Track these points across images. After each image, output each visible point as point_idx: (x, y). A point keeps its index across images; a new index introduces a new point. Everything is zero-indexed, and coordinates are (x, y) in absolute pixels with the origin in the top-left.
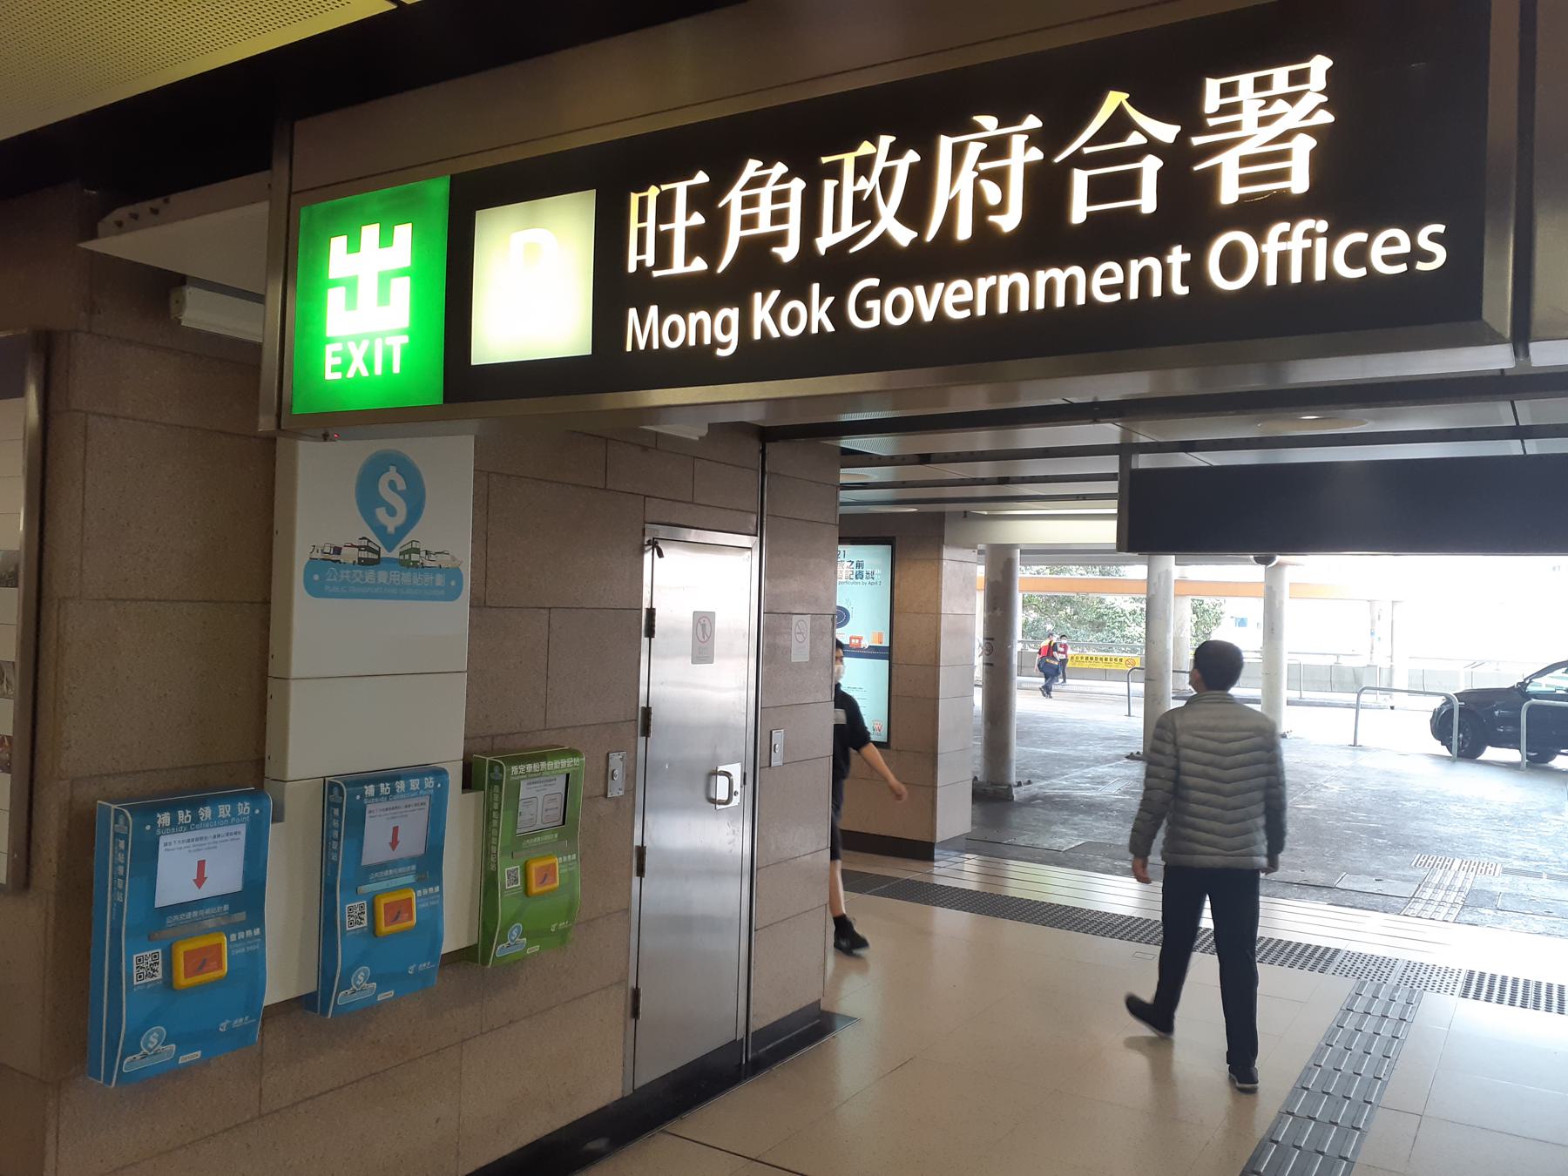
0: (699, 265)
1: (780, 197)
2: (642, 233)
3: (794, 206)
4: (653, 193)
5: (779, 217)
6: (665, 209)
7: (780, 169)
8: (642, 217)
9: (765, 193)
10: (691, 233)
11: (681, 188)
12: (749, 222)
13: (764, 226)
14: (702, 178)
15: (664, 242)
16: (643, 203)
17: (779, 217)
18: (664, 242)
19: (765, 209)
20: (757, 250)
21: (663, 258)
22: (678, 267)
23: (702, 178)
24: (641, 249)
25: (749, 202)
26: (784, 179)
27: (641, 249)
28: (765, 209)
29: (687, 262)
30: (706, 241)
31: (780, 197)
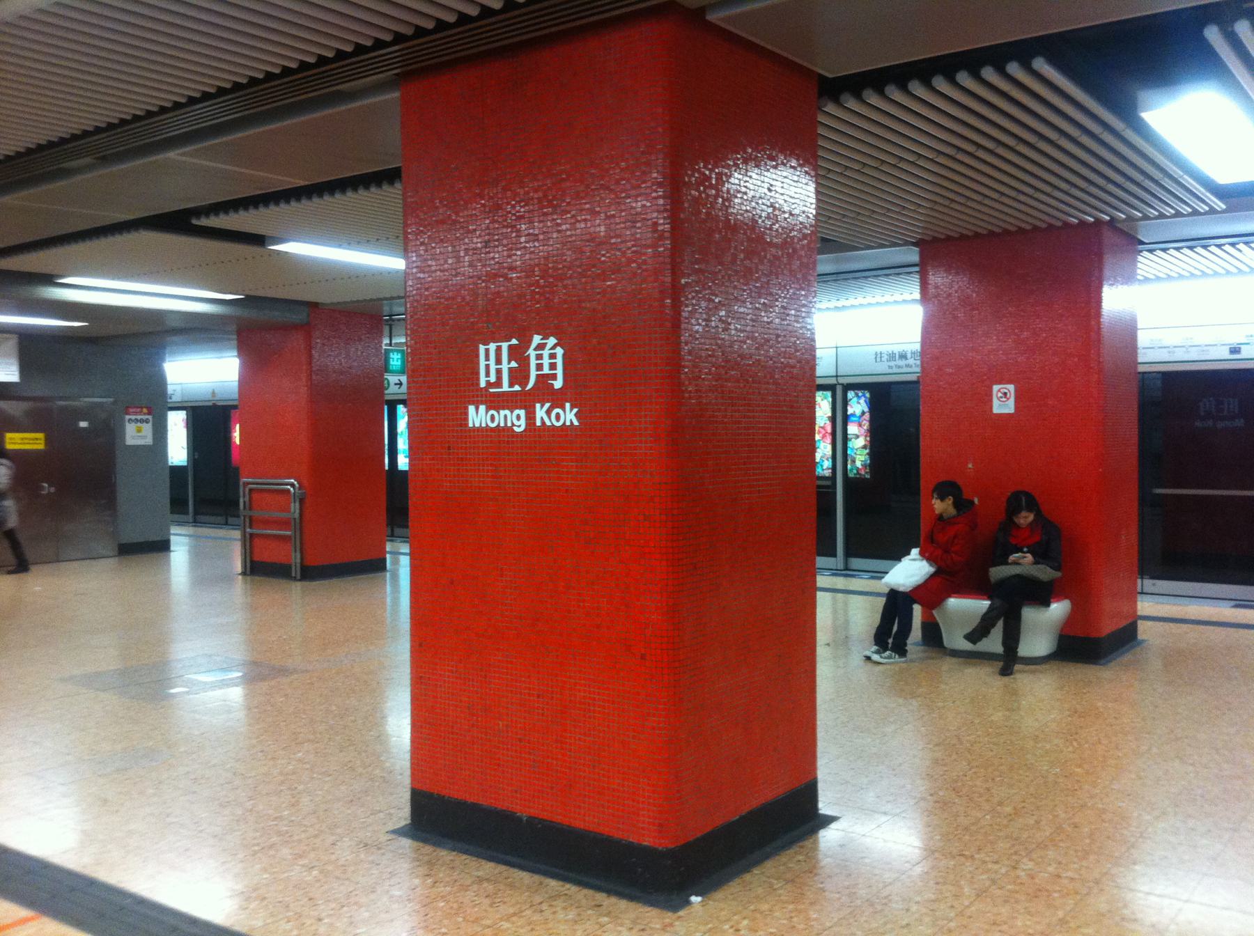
0: (517, 388)
1: (553, 356)
2: (487, 367)
3: (559, 361)
4: (492, 347)
5: (553, 366)
7: (552, 341)
8: (487, 359)
9: (546, 353)
10: (511, 370)
11: (505, 345)
12: (539, 367)
13: (546, 370)
14: (514, 341)
15: (499, 372)
16: (487, 351)
17: (553, 366)
18: (499, 372)
19: (546, 362)
20: (543, 380)
21: (499, 383)
22: (505, 387)
23: (514, 341)
24: (488, 375)
25: (539, 357)
26: (554, 347)
27: (488, 375)
28: (546, 362)
29: (511, 385)
30: (519, 375)
31: (553, 356)
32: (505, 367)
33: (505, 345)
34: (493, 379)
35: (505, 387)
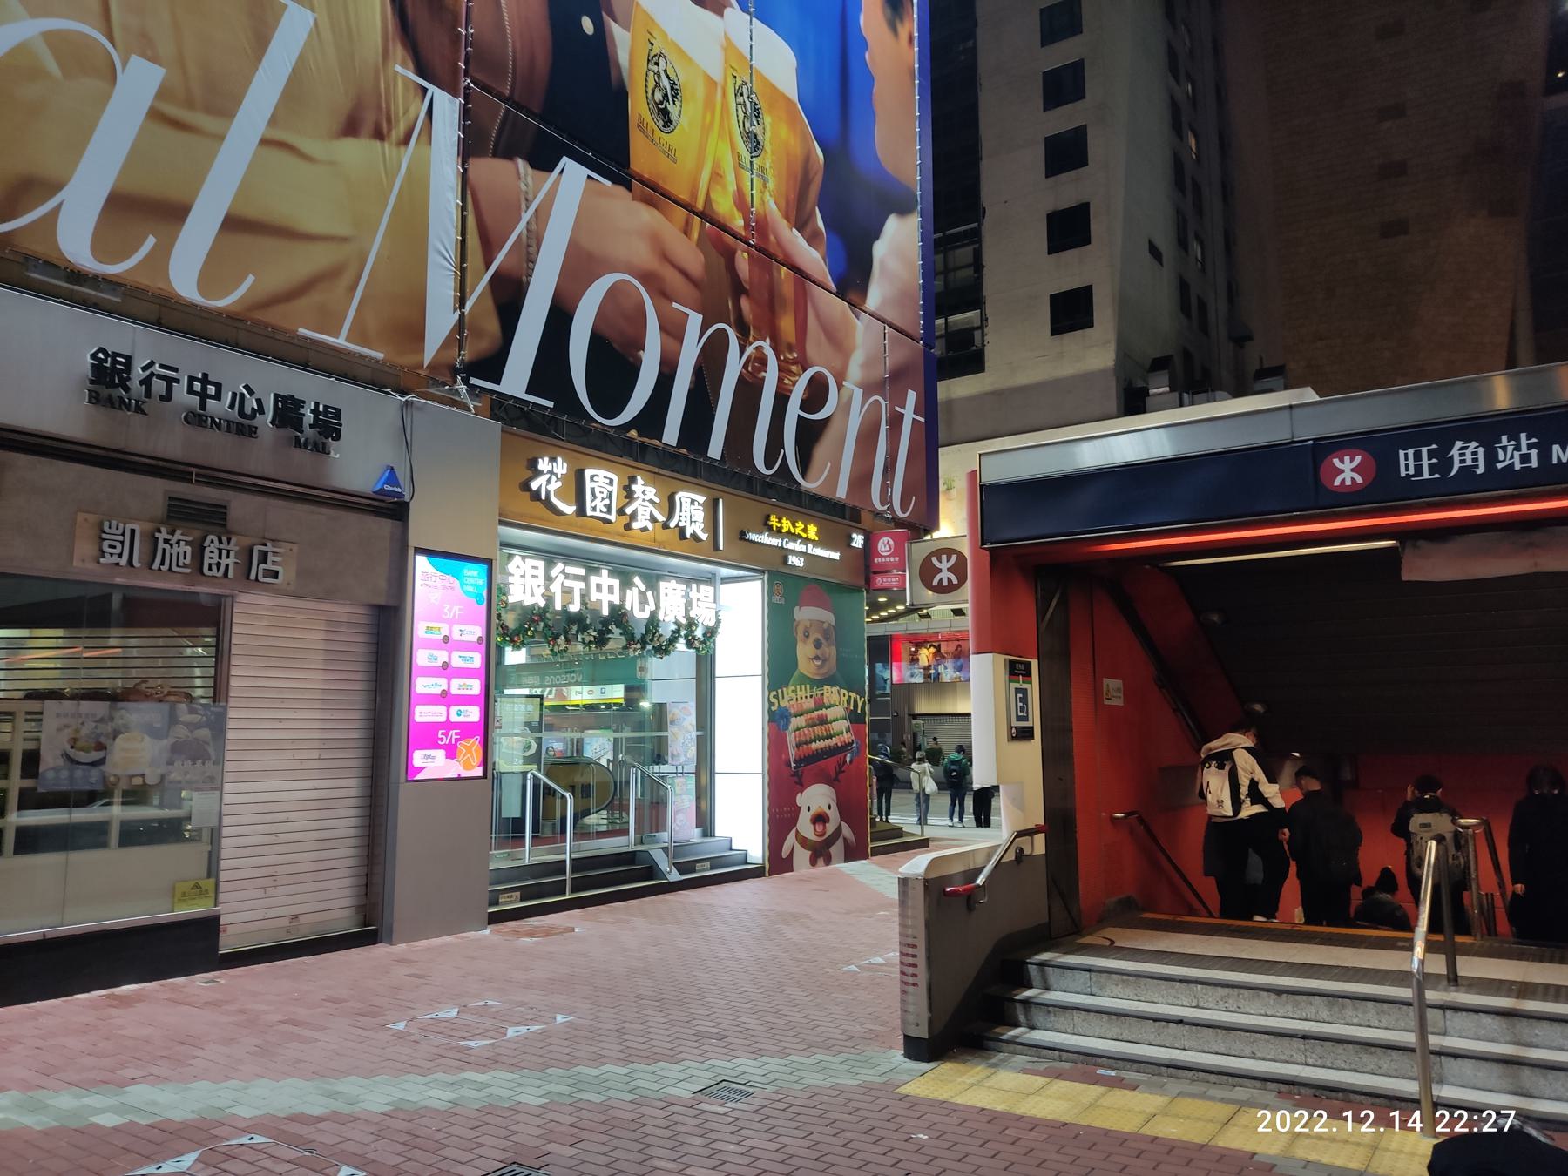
1: (1474, 453)
3: (1481, 456)
4: (1411, 452)
5: (1475, 460)
6: (1418, 456)
7: (1474, 444)
9: (1468, 452)
11: (1424, 450)
13: (1469, 463)
15: (1419, 469)
17: (1475, 460)
18: (1419, 469)
22: (1426, 476)
25: (1462, 455)
32: (1425, 462)
33: (1424, 450)
34: (1412, 472)
35: (1426, 476)
